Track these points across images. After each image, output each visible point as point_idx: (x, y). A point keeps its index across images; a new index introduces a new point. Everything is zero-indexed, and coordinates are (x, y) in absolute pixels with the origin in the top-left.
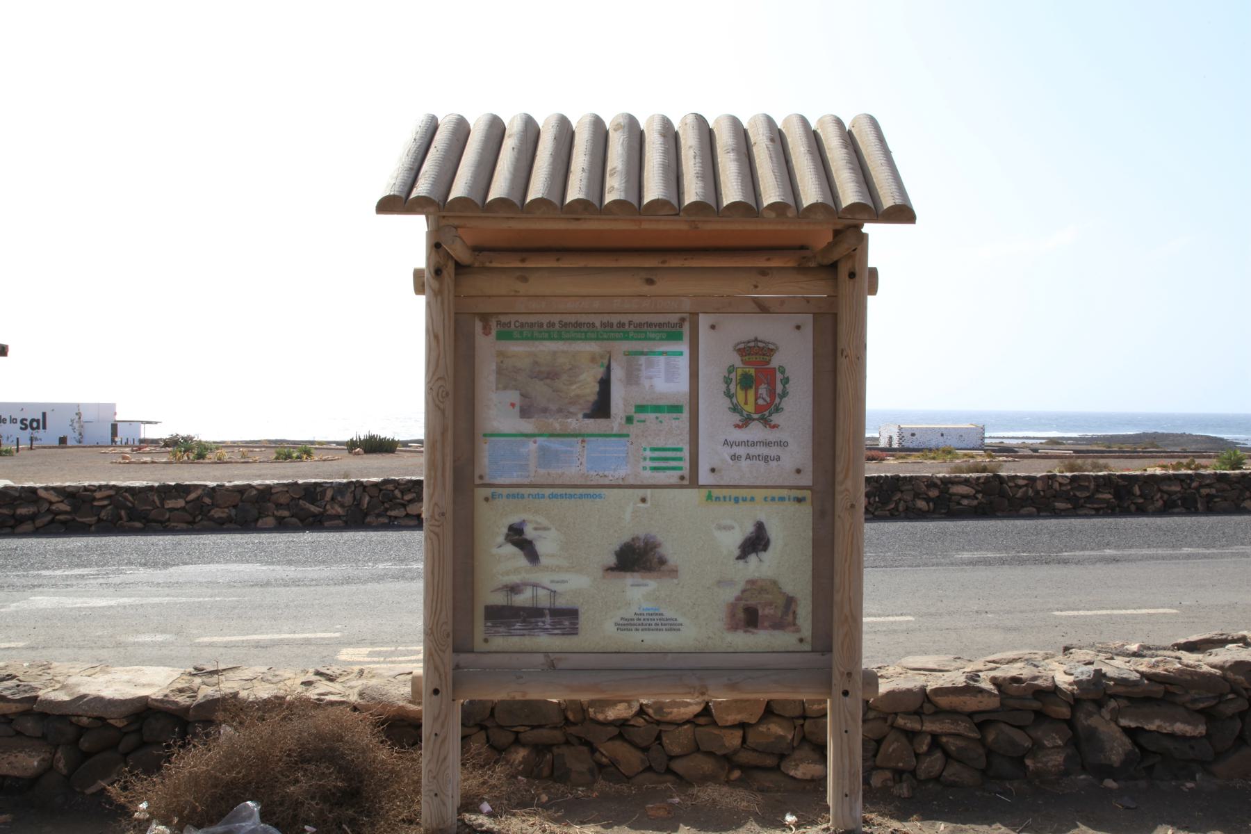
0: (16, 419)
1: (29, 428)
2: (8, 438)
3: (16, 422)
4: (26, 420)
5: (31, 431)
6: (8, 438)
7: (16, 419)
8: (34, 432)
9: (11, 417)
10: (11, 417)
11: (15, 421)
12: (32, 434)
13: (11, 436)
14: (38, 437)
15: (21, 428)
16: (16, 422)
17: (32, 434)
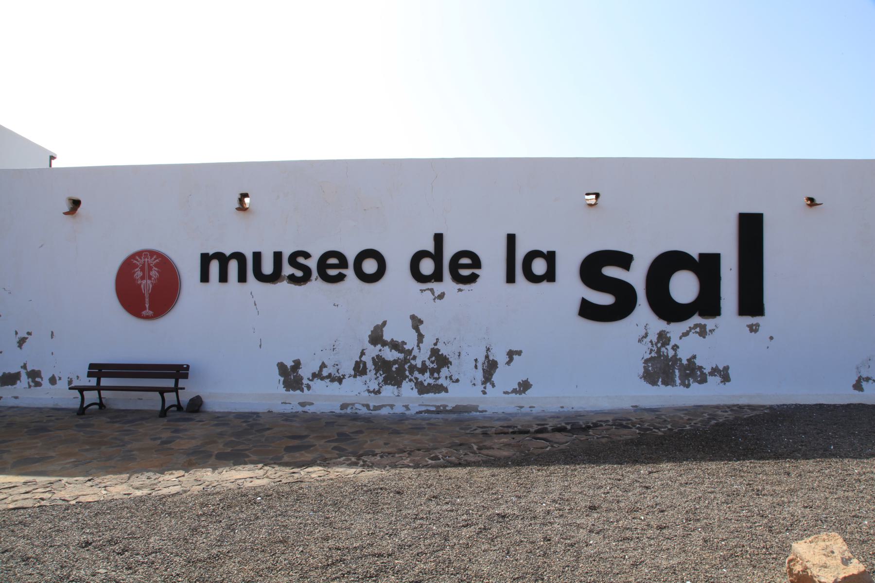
0: (550, 258)
1: (643, 310)
2: (490, 367)
3: (550, 276)
4: (624, 260)
5: (657, 325)
6: (490, 367)
7: (550, 258)
8: (675, 329)
9: (511, 239)
10: (511, 239)
11: (539, 267)
12: (663, 338)
13: (511, 354)
14: (705, 362)
15: (588, 311)
16: (550, 276)
17: (663, 338)
